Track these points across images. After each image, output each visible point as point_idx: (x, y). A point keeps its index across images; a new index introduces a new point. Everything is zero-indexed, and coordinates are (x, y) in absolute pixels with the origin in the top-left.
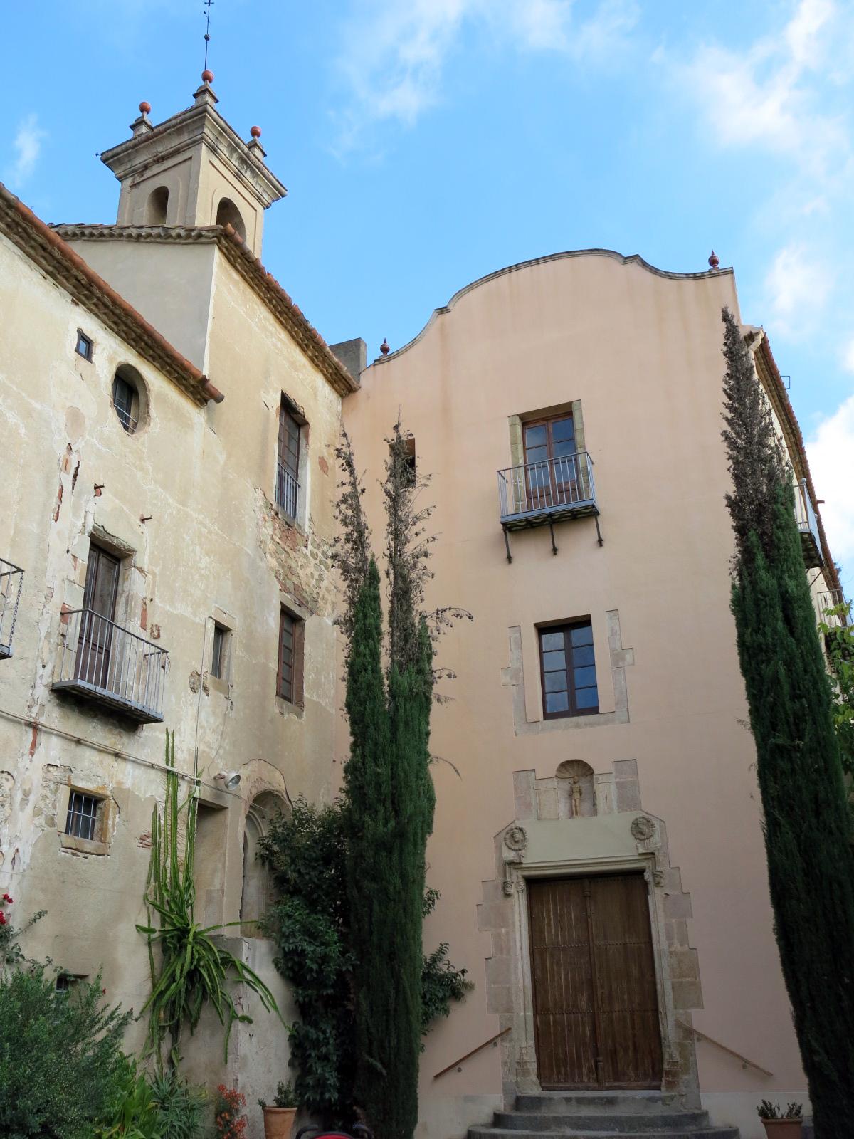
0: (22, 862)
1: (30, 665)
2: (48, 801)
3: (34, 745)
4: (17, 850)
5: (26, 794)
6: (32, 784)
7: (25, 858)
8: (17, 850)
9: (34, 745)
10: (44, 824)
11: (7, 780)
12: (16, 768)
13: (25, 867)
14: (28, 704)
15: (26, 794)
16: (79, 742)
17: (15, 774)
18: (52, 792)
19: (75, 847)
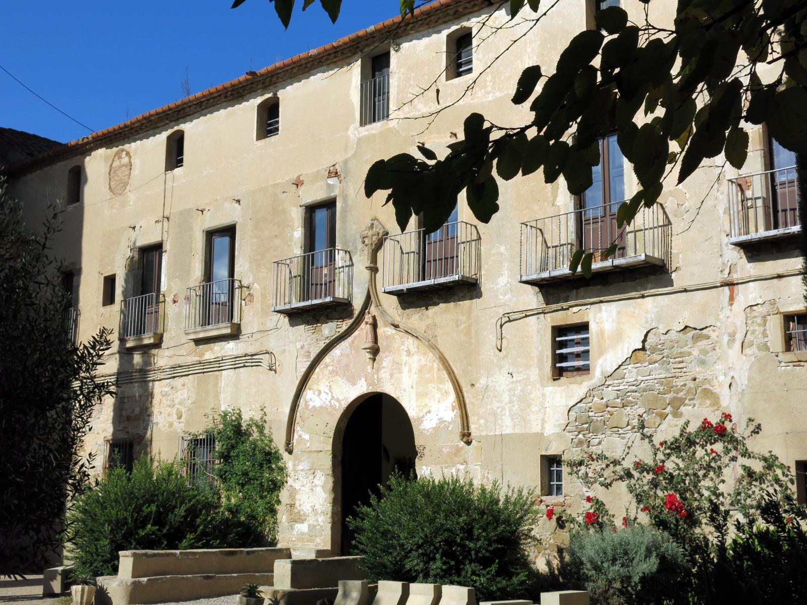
0: (740, 385)
1: (715, 241)
2: (757, 333)
3: (732, 299)
4: (733, 377)
5: (732, 336)
6: (736, 327)
7: (742, 380)
8: (733, 377)
9: (732, 299)
10: (756, 351)
11: (714, 331)
12: (718, 319)
13: (744, 387)
14: (720, 269)
15: (732, 336)
16: (780, 277)
17: (718, 324)
18: (759, 325)
19: (797, 360)
